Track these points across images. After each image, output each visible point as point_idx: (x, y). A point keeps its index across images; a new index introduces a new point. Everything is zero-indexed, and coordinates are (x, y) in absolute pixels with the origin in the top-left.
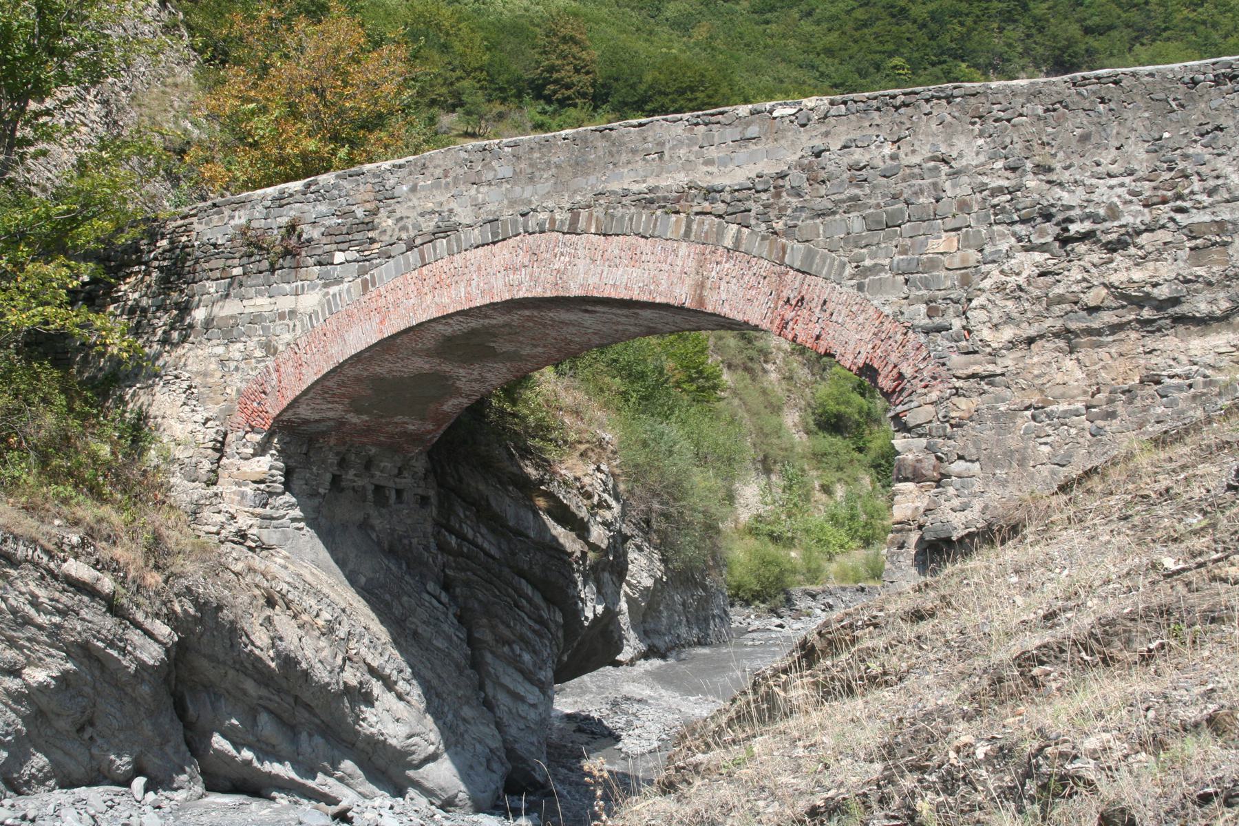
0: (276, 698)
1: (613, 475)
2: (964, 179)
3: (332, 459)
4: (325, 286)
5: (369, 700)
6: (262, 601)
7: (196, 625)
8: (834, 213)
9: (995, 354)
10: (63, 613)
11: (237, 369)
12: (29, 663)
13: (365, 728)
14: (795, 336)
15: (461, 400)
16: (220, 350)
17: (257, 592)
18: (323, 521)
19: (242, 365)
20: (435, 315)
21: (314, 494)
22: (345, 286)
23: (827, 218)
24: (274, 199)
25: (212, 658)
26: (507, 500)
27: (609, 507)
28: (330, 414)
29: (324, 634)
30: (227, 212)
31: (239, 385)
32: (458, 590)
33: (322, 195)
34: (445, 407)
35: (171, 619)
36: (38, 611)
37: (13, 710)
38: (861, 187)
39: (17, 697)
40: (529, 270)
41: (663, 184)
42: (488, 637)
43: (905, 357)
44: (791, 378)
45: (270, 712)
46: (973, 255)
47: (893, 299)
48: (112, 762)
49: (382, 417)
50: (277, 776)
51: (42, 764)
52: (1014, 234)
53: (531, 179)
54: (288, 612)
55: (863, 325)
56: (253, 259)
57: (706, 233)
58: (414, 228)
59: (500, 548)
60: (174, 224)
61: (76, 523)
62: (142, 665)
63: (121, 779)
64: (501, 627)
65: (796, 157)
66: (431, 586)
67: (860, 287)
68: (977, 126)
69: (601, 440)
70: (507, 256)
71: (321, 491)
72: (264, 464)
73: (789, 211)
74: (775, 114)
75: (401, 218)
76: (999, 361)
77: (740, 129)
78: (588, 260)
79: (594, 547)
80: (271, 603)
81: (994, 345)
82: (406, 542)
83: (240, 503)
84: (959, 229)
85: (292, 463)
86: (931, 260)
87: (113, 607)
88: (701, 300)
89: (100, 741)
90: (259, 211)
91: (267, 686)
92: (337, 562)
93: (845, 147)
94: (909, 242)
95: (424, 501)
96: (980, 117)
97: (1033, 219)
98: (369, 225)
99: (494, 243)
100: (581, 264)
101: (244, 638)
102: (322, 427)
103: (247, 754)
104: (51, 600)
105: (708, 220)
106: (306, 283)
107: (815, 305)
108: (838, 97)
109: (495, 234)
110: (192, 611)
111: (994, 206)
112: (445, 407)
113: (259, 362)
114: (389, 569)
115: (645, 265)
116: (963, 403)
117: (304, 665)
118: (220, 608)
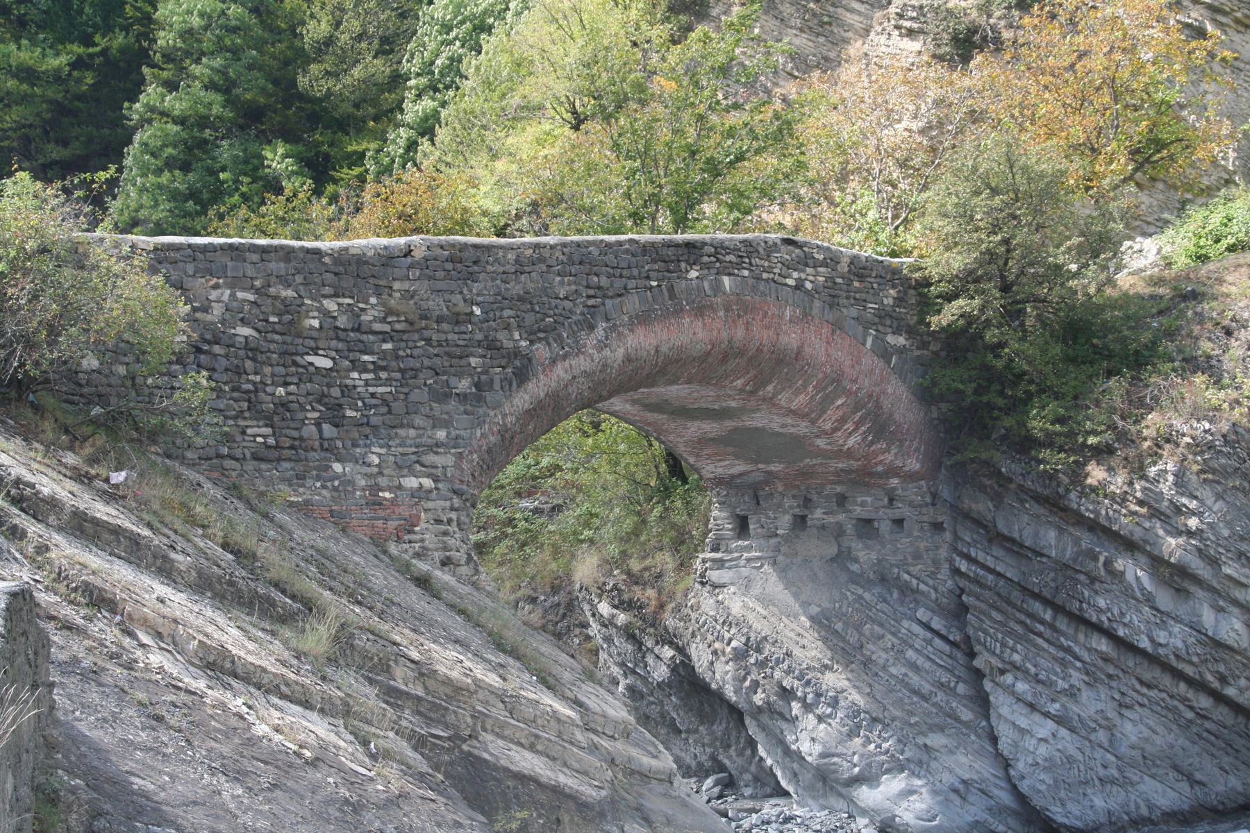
3: (788, 502)
18: (780, 558)
26: (1026, 518)
66: (921, 614)
85: (738, 511)
114: (861, 597)
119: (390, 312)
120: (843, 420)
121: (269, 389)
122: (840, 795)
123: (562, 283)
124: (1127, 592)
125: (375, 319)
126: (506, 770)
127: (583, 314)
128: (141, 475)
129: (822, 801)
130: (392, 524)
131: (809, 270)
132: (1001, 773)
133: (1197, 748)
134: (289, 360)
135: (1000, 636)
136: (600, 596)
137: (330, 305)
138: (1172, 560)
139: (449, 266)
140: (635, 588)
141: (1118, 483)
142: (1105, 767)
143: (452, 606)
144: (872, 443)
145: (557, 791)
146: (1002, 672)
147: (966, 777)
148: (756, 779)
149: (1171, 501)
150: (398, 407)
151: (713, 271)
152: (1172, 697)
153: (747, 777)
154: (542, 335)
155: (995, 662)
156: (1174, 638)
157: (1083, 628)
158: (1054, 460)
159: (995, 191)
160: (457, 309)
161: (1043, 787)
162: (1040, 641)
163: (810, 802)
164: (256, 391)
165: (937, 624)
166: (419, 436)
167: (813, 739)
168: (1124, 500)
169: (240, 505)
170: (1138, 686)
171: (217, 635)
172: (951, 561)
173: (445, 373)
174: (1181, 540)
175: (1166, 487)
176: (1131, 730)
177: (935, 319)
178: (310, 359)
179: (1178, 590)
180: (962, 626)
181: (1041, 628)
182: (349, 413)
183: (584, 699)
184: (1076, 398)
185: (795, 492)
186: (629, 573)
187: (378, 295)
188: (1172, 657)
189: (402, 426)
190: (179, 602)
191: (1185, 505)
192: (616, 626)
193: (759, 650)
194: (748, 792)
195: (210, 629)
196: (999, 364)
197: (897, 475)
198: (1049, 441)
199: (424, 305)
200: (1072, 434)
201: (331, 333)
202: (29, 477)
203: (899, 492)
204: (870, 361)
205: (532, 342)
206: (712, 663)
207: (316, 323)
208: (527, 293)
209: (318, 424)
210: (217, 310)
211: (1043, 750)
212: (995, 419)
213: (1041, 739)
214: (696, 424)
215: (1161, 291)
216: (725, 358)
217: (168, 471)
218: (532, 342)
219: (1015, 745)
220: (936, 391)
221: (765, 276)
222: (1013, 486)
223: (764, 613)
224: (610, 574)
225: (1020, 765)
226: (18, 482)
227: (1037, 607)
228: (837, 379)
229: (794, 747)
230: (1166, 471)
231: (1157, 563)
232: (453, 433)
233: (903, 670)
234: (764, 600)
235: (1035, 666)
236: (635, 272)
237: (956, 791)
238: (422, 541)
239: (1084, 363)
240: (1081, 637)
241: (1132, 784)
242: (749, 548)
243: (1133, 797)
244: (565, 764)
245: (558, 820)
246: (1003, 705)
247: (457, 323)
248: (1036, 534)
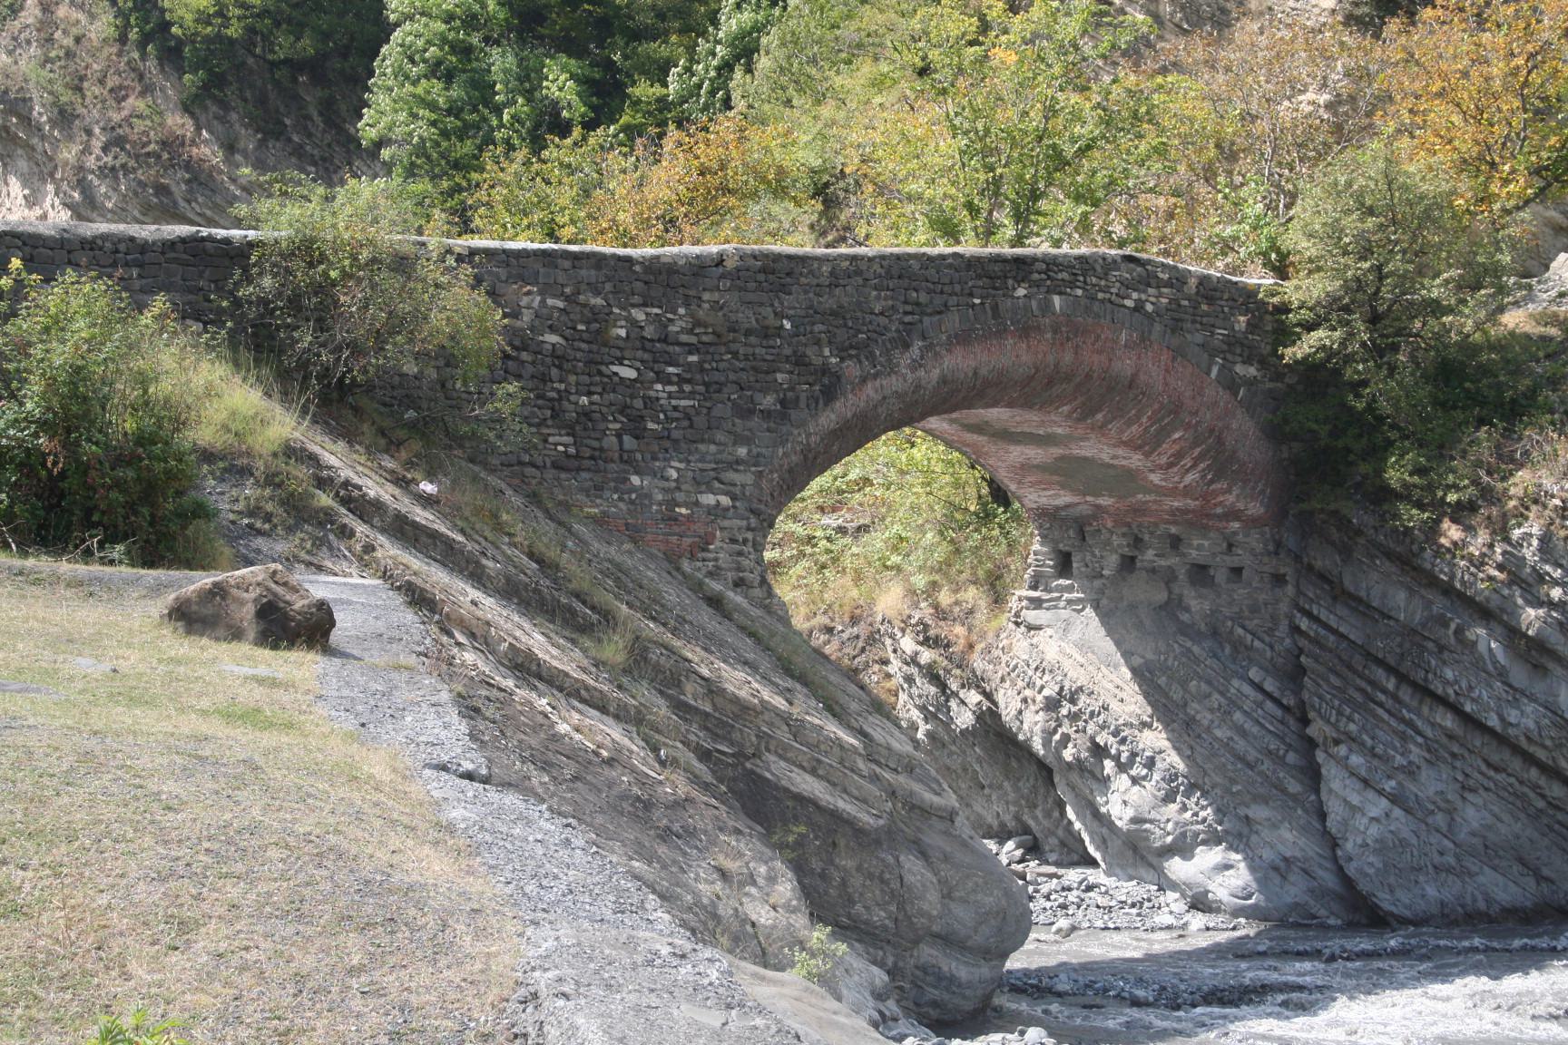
3: (1116, 541)
18: (1104, 602)
26: (1375, 576)
66: (1254, 673)
119: (698, 323)
120: (1179, 456)
121: (573, 398)
122: (1151, 865)
123: (878, 298)
124: (1478, 664)
125: (683, 330)
126: (787, 790)
127: (898, 331)
128: (454, 482)
129: (1131, 871)
130: (687, 541)
131: (1150, 291)
132: (1328, 853)
133: (1546, 842)
134: (594, 369)
135: (1337, 703)
136: (903, 631)
137: (639, 315)
138: (1530, 633)
139: (761, 277)
140: (942, 623)
141: (1477, 545)
142: (1441, 854)
143: (742, 628)
144: (1212, 482)
145: (835, 815)
146: (1337, 742)
147: (1288, 854)
148: (1063, 844)
149: (1533, 568)
150: (700, 421)
151: (1043, 289)
152: (1521, 783)
153: (1053, 841)
154: (853, 352)
155: (1328, 730)
156: (1525, 718)
157: (1428, 700)
158: (1413, 517)
159: (1371, 211)
160: (766, 323)
161: (1371, 871)
162: (1380, 711)
163: (1118, 871)
164: (560, 399)
165: (1269, 686)
166: (720, 452)
167: (1125, 802)
168: (1483, 564)
169: (540, 514)
170: (1484, 768)
171: (524, 639)
172: (1291, 618)
173: (750, 388)
174: (1541, 612)
175: (1530, 553)
176: (1473, 815)
177: (1289, 351)
178: (615, 368)
179: (1535, 666)
180: (1298, 688)
181: (1381, 697)
182: (651, 425)
183: (869, 730)
184: (1441, 447)
185: (1125, 530)
186: (936, 607)
187: (687, 305)
188: (1522, 738)
189: (703, 441)
190: (490, 607)
192: (918, 665)
193: (1073, 701)
194: (1053, 857)
195: (518, 633)
196: (1360, 405)
197: (1238, 519)
198: (1405, 495)
199: (733, 317)
200: (1430, 488)
201: (638, 343)
202: (356, 480)
203: (1240, 537)
204: (1214, 392)
205: (842, 359)
206: (1020, 712)
207: (623, 333)
208: (841, 307)
209: (619, 436)
210: (527, 316)
211: (1374, 830)
212: (1351, 463)
213: (1373, 819)
214: (1019, 448)
215: (1553, 331)
216: (1050, 383)
217: (475, 479)
218: (842, 359)
219: (1345, 823)
220: (1287, 429)
221: (1100, 296)
222: (1362, 541)
223: (1082, 660)
224: (916, 606)
225: (1349, 846)
226: (347, 483)
227: (1380, 674)
228: (1176, 408)
229: (1103, 810)
230: (1531, 535)
231: (1513, 634)
232: (755, 451)
233: (1229, 734)
234: (1082, 646)
235: (1373, 738)
236: (957, 288)
237: (1276, 869)
238: (716, 560)
239: (1455, 407)
240: (1425, 710)
241: (1471, 875)
242: (1070, 589)
243: (1470, 889)
244: (845, 791)
245: (834, 843)
246: (1336, 782)
247: (766, 337)
248: (1384, 596)
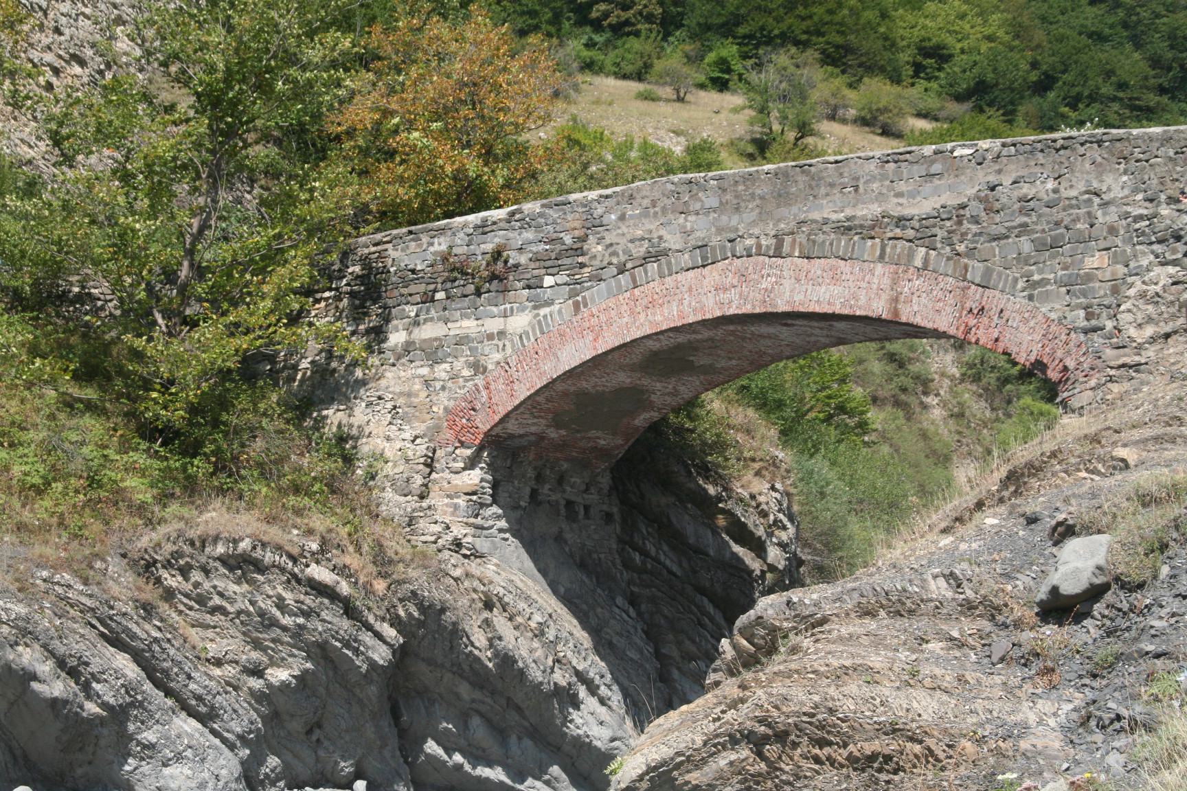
0: (489, 700)
1: (788, 495)
2: (1112, 209)
3: (531, 474)
4: (535, 308)
5: (576, 704)
6: (481, 605)
7: (419, 628)
8: (1007, 237)
9: (1139, 348)
10: (307, 614)
11: (443, 388)
12: (273, 663)
13: (572, 730)
14: (978, 340)
15: (653, 413)
16: (425, 371)
17: (475, 596)
19: (449, 384)
20: (649, 332)
21: (516, 507)
22: (556, 307)
23: (1002, 242)
24: (476, 227)
25: (431, 662)
26: (687, 517)
27: (784, 528)
28: (533, 429)
29: (536, 636)
30: (425, 239)
31: (446, 403)
32: (643, 607)
33: (528, 223)
34: (636, 422)
35: (395, 622)
36: (283, 613)
37: (255, 710)
38: (1029, 215)
39: (258, 697)
40: (739, 289)
41: (859, 213)
42: (675, 653)
43: (1069, 353)
44: (961, 415)
45: (482, 715)
46: (1121, 270)
47: (1057, 306)
48: (336, 763)
49: (578, 431)
50: (487, 779)
51: (274, 764)
52: (1152, 252)
53: (737, 209)
54: (506, 614)
55: (1033, 328)
56: (457, 283)
57: (899, 255)
58: (624, 253)
59: (681, 566)
60: (366, 251)
61: (310, 532)
62: (373, 664)
63: (344, 781)
64: (687, 642)
65: (974, 191)
66: (619, 600)
67: (1031, 298)
68: (1122, 166)
69: (774, 458)
70: (717, 277)
71: (523, 504)
72: (475, 477)
73: (970, 236)
74: (955, 154)
75: (611, 245)
76: (1143, 353)
77: (925, 166)
78: (793, 280)
79: (772, 568)
80: (489, 606)
81: (1139, 340)
82: (595, 556)
83: (453, 514)
84: (1109, 249)
86: (1087, 274)
87: (350, 610)
88: (896, 312)
89: (326, 743)
90: (460, 238)
91: (482, 688)
92: (539, 571)
93: (1015, 182)
94: (1069, 260)
95: (608, 517)
96: (1125, 158)
97: (1167, 240)
98: (580, 252)
99: (704, 266)
100: (787, 284)
101: (465, 639)
102: (524, 442)
103: (458, 758)
104: (297, 602)
105: (900, 243)
106: (515, 306)
107: (994, 312)
108: (1009, 140)
109: (704, 258)
110: (416, 614)
111: (1136, 230)
112: (636, 422)
113: (467, 381)
115: (845, 284)
116: (1116, 388)
117: (521, 664)
118: (443, 610)
191: (781, 521)
